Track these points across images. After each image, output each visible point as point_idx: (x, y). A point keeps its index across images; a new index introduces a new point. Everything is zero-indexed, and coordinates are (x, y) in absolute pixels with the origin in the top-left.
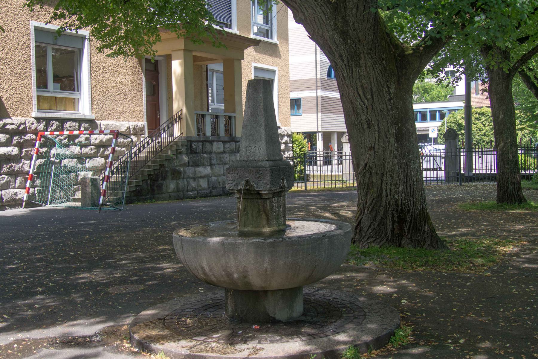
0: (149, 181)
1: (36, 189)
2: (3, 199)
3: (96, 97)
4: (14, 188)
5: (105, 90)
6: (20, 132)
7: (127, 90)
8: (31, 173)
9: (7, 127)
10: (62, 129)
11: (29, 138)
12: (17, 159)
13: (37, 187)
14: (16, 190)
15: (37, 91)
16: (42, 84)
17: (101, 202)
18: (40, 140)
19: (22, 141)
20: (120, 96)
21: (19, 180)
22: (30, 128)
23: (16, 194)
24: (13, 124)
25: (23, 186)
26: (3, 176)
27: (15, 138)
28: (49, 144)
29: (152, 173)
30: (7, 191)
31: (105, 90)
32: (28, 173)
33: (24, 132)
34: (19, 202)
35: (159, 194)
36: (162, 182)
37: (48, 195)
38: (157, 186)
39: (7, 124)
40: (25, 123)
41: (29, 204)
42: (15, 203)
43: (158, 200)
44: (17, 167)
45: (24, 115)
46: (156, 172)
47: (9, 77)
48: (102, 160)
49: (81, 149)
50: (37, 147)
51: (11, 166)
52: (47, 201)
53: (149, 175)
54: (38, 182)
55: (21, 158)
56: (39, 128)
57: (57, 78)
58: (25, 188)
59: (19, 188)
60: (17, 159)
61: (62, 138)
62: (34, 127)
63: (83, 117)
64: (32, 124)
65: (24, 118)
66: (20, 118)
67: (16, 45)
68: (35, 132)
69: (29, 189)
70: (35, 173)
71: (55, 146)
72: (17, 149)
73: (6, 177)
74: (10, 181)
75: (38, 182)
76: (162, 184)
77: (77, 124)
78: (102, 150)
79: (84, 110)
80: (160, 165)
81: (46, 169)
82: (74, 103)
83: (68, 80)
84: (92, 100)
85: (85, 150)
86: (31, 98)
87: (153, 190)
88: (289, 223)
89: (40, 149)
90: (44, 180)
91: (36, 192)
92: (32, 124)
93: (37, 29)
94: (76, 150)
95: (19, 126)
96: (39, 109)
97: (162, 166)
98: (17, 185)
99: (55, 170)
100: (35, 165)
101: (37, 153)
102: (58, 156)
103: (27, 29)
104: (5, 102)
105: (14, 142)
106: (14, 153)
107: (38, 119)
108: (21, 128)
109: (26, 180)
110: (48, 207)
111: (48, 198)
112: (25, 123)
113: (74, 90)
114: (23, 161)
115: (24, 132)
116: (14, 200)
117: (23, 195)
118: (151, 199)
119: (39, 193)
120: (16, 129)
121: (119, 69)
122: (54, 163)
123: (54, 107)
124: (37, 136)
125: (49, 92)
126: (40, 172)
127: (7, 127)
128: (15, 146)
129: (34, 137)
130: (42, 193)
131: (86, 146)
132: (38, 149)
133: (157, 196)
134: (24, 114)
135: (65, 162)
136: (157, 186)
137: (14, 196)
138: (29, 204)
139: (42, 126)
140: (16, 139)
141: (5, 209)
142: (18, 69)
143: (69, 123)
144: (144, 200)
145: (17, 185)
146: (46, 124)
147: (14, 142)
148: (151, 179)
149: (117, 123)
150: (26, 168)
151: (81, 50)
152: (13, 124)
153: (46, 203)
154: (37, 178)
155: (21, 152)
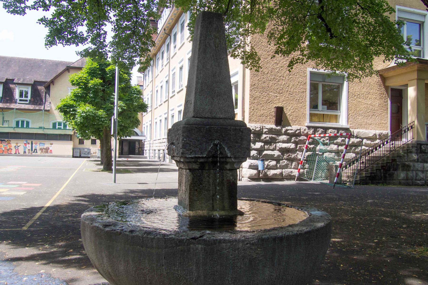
0: (382, 171)
1: (305, 170)
2: (283, 175)
3: (351, 114)
4: (291, 168)
5: (358, 109)
6: (296, 135)
7: (376, 109)
8: (301, 160)
9: (288, 132)
10: (325, 133)
11: (302, 139)
12: (293, 151)
13: (306, 169)
14: (291, 170)
15: (310, 110)
16: (314, 106)
17: (335, 181)
18: (309, 140)
19: (297, 140)
20: (369, 113)
21: (294, 164)
22: (303, 133)
23: (291, 172)
24: (292, 130)
25: (296, 168)
26: (284, 160)
27: (293, 138)
28: (315, 143)
29: (385, 165)
30: (286, 170)
31: (358, 109)
32: (300, 160)
33: (299, 135)
34: (294, 177)
35: (390, 180)
36: (393, 172)
37: (312, 174)
38: (389, 175)
39: (289, 130)
40: (300, 129)
41: (299, 179)
42: (290, 177)
43: (389, 184)
44: (293, 156)
45: (300, 124)
46: (388, 164)
47: (291, 102)
48: (354, 155)
49: (338, 147)
50: (306, 144)
51: (290, 155)
52: (311, 178)
53: (382, 167)
54: (307, 166)
55: (296, 151)
56: (309, 133)
57: (325, 102)
58: (297, 169)
59: (294, 168)
60: (293, 151)
61: (325, 139)
62: (306, 132)
63: (341, 127)
64: (305, 130)
65: (300, 126)
66: (297, 126)
67: (297, 83)
68: (307, 135)
69: (300, 169)
70: (305, 160)
71: (319, 144)
72: (294, 145)
73: (286, 161)
74: (288, 164)
75: (307, 166)
76: (393, 174)
77: (336, 131)
78: (354, 148)
79: (343, 122)
80: (392, 160)
81: (312, 158)
82: (336, 118)
83: (333, 104)
84: (348, 116)
85: (340, 148)
86: (305, 114)
87: (385, 177)
88: (219, 216)
89: (309, 145)
90: (310, 164)
91: (305, 172)
92: (305, 130)
93: (311, 73)
94: (334, 147)
95: (296, 131)
96: (311, 121)
97: (394, 160)
98: (293, 167)
99: (318, 159)
100: (304, 155)
101: (306, 148)
102: (320, 150)
103: (305, 73)
104: (288, 117)
105: (292, 141)
106: (291, 147)
107: (309, 127)
108: (297, 132)
109: (298, 164)
110: (312, 182)
111: (312, 177)
112: (300, 129)
113: (337, 110)
114: (298, 152)
115: (299, 135)
116: (290, 175)
117: (296, 173)
118: (383, 183)
119: (307, 172)
120: (294, 133)
121: (370, 96)
122: (317, 154)
123: (322, 120)
124: (307, 137)
125: (319, 111)
126: (309, 160)
127: (288, 132)
128: (293, 143)
129: (306, 138)
130: (309, 173)
131: (342, 145)
132: (307, 146)
133: (388, 181)
134: (300, 124)
135: (326, 155)
136: (389, 175)
137: (290, 173)
138: (299, 179)
139: (311, 131)
140: (293, 139)
141: (284, 181)
142: (297, 97)
143: (330, 130)
144: (377, 184)
145: (293, 167)
146: (314, 130)
147: (292, 141)
148: (384, 169)
149: (367, 131)
150: (299, 157)
151: (342, 84)
152: (292, 130)
153: (311, 179)
154: (306, 163)
155: (296, 147)
